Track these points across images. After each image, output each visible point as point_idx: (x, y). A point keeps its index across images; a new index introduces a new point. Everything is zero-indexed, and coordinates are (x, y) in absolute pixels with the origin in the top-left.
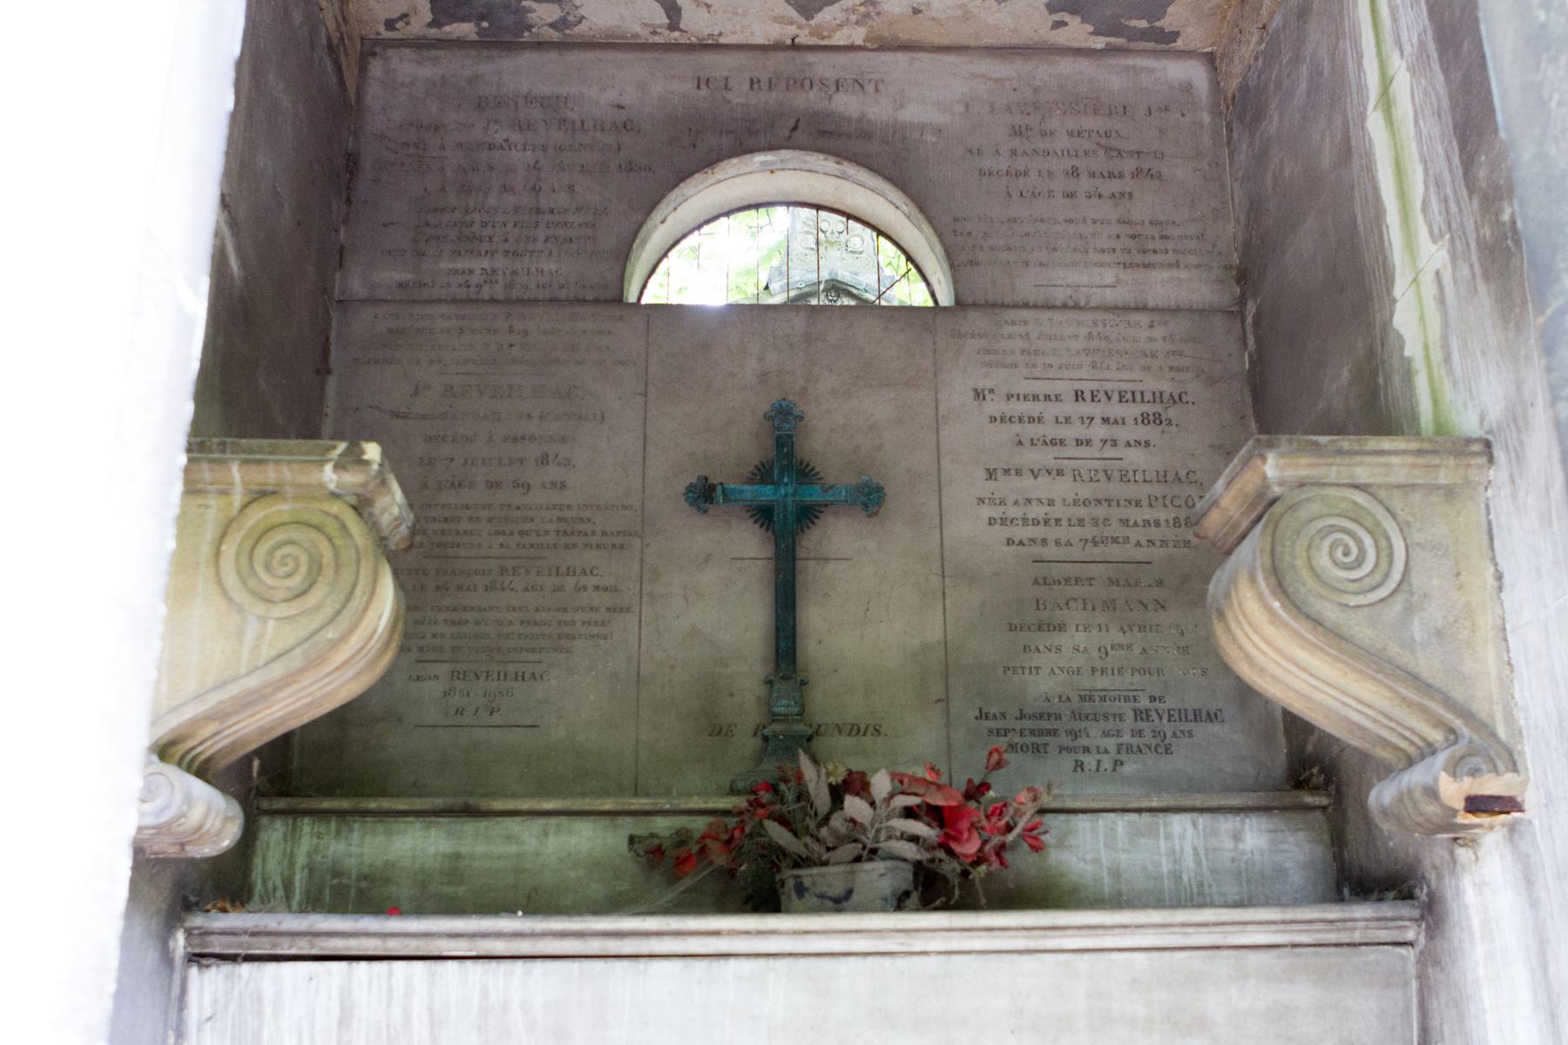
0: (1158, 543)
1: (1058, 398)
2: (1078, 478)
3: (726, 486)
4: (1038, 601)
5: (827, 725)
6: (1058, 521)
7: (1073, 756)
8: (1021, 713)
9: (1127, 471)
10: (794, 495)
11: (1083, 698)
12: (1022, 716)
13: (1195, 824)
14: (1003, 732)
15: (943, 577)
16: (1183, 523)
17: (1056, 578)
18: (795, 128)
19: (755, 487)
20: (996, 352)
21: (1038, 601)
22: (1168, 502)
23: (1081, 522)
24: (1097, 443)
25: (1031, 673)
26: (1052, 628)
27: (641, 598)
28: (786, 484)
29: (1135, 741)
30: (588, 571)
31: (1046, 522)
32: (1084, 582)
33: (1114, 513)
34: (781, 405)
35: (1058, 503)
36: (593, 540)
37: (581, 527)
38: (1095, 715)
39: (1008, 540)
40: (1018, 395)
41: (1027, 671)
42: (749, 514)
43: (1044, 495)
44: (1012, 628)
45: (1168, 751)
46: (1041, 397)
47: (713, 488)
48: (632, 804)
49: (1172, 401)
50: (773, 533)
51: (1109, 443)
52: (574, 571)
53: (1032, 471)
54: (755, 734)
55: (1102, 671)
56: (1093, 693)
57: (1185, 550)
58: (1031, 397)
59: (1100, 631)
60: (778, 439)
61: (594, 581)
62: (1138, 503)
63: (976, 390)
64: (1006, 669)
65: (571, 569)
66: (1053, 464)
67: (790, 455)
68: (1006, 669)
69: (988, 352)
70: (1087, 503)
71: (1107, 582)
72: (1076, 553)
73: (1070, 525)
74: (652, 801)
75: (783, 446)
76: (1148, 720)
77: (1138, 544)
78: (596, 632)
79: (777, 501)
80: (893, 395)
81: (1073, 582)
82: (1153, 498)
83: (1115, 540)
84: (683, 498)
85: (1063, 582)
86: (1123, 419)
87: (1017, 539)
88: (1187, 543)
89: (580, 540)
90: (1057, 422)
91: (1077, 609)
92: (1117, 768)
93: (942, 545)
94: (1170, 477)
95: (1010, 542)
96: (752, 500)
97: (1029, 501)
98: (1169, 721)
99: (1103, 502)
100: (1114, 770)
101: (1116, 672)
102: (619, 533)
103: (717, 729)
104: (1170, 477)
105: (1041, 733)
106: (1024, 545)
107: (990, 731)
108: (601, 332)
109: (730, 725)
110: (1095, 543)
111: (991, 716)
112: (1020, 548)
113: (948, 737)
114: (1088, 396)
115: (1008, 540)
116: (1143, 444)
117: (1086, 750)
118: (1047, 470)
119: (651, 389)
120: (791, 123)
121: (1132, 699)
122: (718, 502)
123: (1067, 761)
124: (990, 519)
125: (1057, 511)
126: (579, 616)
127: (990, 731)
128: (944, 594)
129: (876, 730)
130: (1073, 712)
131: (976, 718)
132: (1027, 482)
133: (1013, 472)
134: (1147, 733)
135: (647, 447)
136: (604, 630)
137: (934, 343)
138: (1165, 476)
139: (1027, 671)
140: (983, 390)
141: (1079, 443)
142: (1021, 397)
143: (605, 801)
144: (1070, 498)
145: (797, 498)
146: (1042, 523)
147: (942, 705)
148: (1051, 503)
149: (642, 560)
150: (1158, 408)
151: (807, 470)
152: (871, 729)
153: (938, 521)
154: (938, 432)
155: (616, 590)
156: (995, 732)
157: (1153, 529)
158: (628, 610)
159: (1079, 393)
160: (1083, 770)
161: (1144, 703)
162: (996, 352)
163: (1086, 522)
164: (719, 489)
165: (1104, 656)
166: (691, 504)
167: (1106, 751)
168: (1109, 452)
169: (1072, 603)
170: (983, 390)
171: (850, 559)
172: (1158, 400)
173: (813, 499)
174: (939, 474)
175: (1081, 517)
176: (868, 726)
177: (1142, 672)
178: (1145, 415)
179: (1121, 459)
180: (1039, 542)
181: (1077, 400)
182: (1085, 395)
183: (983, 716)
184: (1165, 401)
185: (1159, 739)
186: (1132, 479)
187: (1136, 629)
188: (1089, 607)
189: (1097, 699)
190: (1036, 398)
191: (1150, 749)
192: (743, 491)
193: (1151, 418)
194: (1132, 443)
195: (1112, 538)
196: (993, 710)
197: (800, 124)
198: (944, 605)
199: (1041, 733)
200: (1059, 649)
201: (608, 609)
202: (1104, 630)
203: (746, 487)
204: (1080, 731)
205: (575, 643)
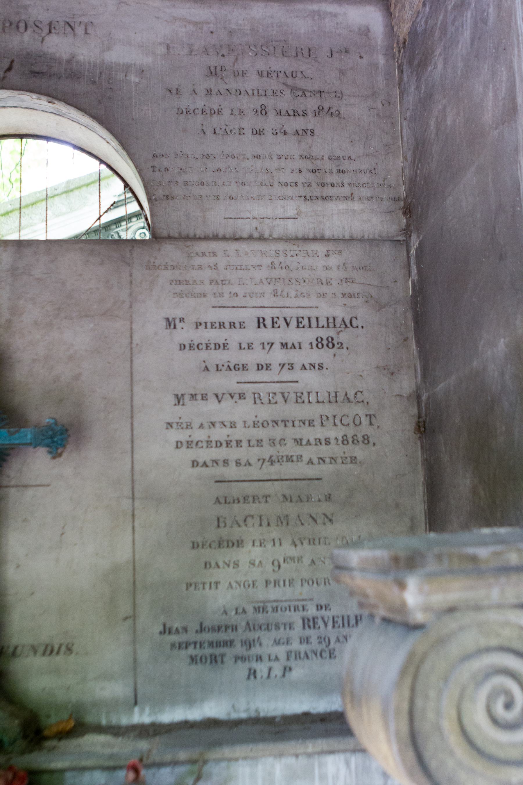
0: (327, 460)
1: (242, 325)
2: (258, 401)
4: (218, 519)
6: (239, 443)
7: (247, 665)
9: (302, 393)
11: (257, 610)
12: (202, 629)
13: (347, 763)
14: (184, 645)
15: (133, 499)
16: (350, 441)
17: (236, 497)
18: (9, 69)
20: (187, 282)
21: (218, 519)
22: (338, 422)
23: (259, 442)
24: (275, 367)
26: (231, 544)
29: (303, 648)
32: (261, 500)
33: (290, 433)
35: (239, 425)
38: (268, 625)
39: (193, 462)
40: (206, 323)
41: (207, 586)
43: (227, 419)
44: (195, 546)
45: (332, 655)
46: (227, 325)
49: (344, 326)
51: (286, 366)
53: (217, 396)
56: (266, 604)
57: (352, 466)
58: (217, 325)
59: (274, 545)
62: (311, 423)
63: (167, 319)
64: (189, 585)
66: (236, 388)
68: (189, 585)
69: (180, 283)
70: (265, 424)
71: (281, 498)
72: (254, 473)
73: (250, 446)
76: (314, 627)
77: (310, 462)
80: (92, 325)
81: (251, 499)
82: (324, 418)
83: (290, 459)
85: (242, 500)
86: (300, 344)
87: (201, 461)
88: (354, 460)
90: (240, 348)
91: (253, 525)
92: (286, 674)
94: (340, 397)
95: (195, 464)
97: (213, 424)
98: (334, 627)
99: (280, 423)
100: (284, 675)
101: (287, 583)
104: (340, 397)
105: (219, 644)
106: (207, 466)
107: (173, 645)
110: (272, 462)
111: (174, 630)
112: (204, 469)
113: (135, 652)
114: (268, 322)
115: (193, 462)
116: (317, 367)
117: (259, 658)
118: (230, 394)
120: (6, 64)
121: (301, 608)
123: (242, 669)
124: (177, 442)
125: (238, 433)
127: (173, 645)
128: (133, 515)
130: (248, 624)
132: (212, 405)
133: (199, 397)
134: (314, 640)
137: (131, 275)
138: (336, 397)
139: (207, 586)
140: (174, 319)
141: (260, 367)
142: (209, 325)
144: (251, 419)
146: (224, 444)
147: (130, 621)
148: (233, 425)
150: (331, 332)
152: (63, 648)
153: (129, 446)
154: (131, 361)
156: (177, 645)
157: (324, 447)
159: (261, 320)
161: (312, 611)
162: (187, 282)
163: (264, 443)
165: (276, 569)
167: (277, 659)
168: (286, 375)
169: (249, 520)
170: (174, 319)
172: (331, 325)
174: (132, 401)
175: (259, 438)
177: (311, 583)
178: (319, 340)
179: (297, 382)
180: (221, 463)
181: (259, 327)
182: (266, 322)
183: (166, 630)
184: (338, 325)
185: (324, 645)
186: (306, 400)
187: (306, 542)
188: (265, 523)
189: (270, 609)
190: (222, 325)
191: (316, 654)
193: (325, 342)
194: (307, 366)
195: (287, 456)
196: (176, 625)
197: (14, 64)
198: (133, 528)
199: (219, 644)
200: (236, 565)
202: (277, 544)
204: (254, 641)
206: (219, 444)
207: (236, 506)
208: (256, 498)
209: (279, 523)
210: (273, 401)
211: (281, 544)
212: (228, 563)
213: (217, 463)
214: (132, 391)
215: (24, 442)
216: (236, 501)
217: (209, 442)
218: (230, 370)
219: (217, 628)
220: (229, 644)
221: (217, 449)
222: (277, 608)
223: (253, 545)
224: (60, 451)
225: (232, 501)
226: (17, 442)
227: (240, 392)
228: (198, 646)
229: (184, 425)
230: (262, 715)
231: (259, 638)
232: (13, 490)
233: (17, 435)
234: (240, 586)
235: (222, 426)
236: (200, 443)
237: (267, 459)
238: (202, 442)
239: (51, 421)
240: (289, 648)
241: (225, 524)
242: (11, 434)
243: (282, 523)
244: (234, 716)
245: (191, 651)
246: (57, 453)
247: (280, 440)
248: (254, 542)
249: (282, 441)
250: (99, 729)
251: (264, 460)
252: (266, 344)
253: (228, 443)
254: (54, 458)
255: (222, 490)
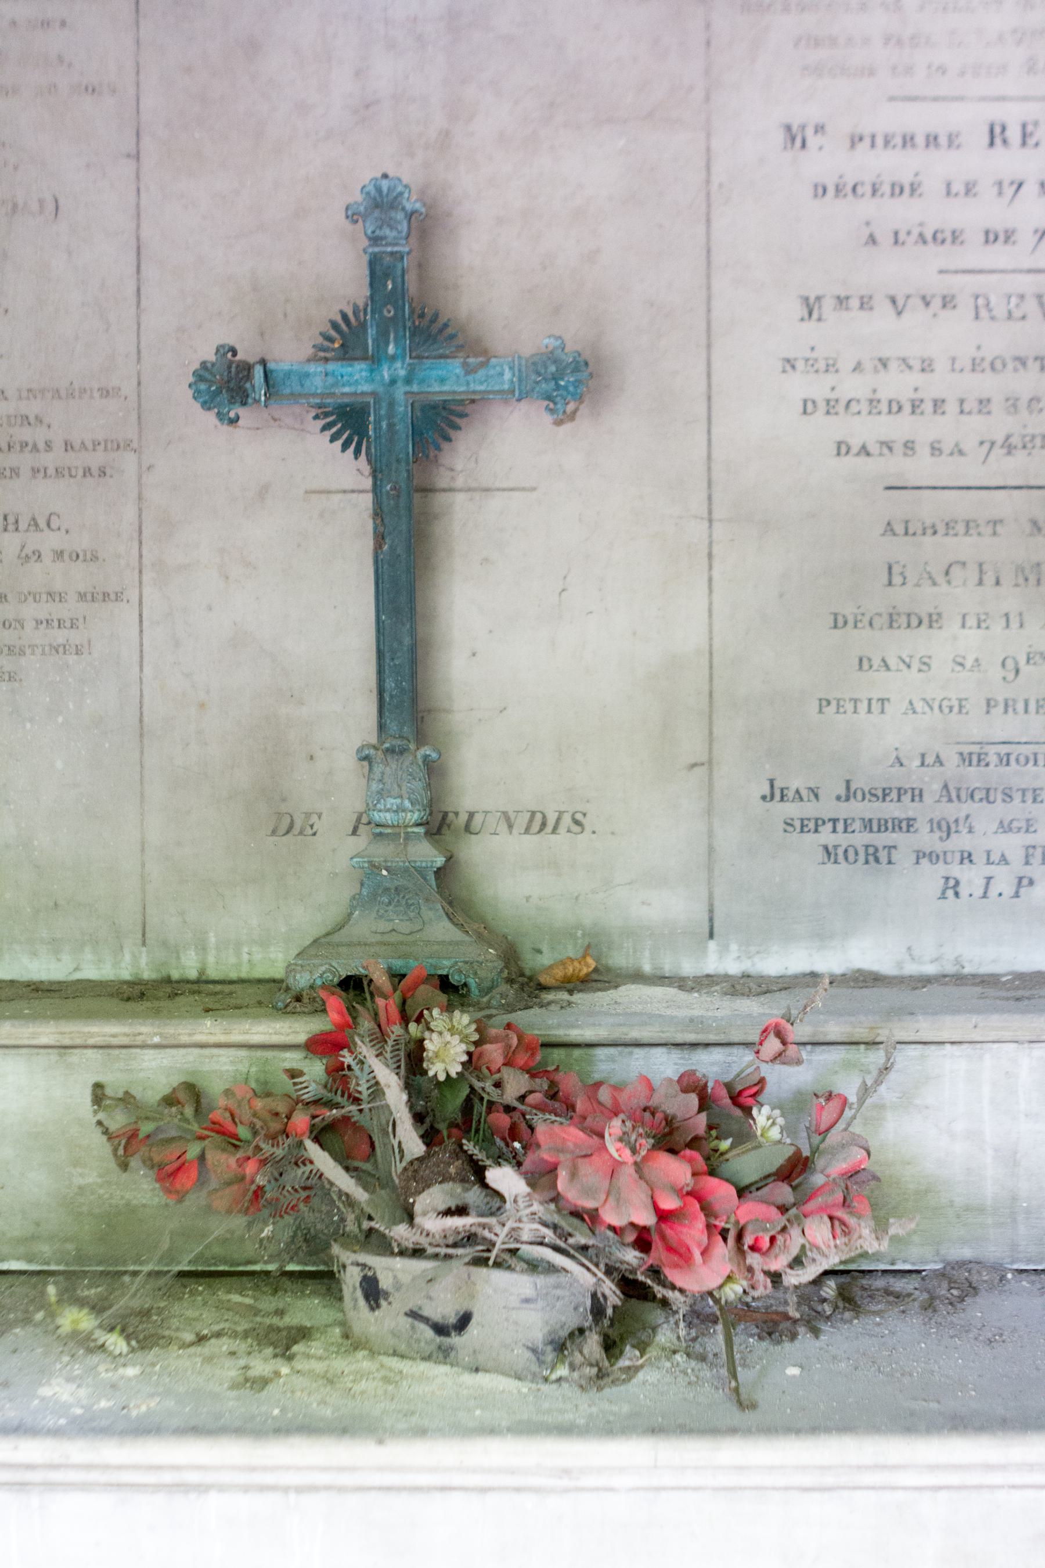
1: (953, 141)
2: (983, 313)
3: (271, 366)
4: (890, 568)
5: (486, 812)
6: (938, 405)
7: (941, 869)
8: (848, 788)
10: (408, 381)
11: (966, 759)
12: (849, 794)
15: (710, 521)
17: (928, 523)
19: (331, 366)
20: (833, 41)
21: (890, 568)
23: (984, 403)
25: (869, 711)
26: (914, 622)
27: (140, 572)
28: (393, 358)
30: (42, 524)
31: (915, 406)
32: (982, 529)
34: (379, 190)
36: (49, 460)
37: (26, 434)
38: (988, 790)
39: (839, 444)
40: (873, 137)
41: (863, 707)
42: (321, 423)
44: (838, 622)
46: (920, 140)
47: (247, 368)
48: (91, 1035)
50: (369, 461)
52: (17, 522)
53: (893, 301)
54: (355, 832)
55: (1006, 706)
56: (988, 748)
58: (898, 140)
59: (1008, 626)
60: (374, 263)
61: (49, 541)
63: (788, 128)
65: (11, 519)
66: (939, 285)
67: (397, 297)
69: (817, 43)
70: (998, 365)
71: (1028, 528)
72: (971, 471)
73: (962, 412)
74: (126, 1029)
75: (386, 276)
78: (61, 641)
79: (374, 394)
80: (622, 143)
81: (961, 528)
84: (190, 393)
87: (856, 445)
89: (25, 461)
90: (948, 193)
91: (964, 584)
92: (1022, 891)
93: (709, 457)
95: (842, 448)
96: (322, 395)
97: (884, 363)
99: (1030, 363)
100: (1017, 895)
101: (1032, 707)
102: (96, 444)
103: (286, 822)
105: (883, 826)
106: (868, 454)
108: (46, 24)
109: (308, 815)
110: (1010, 449)
111: (791, 794)
112: (862, 459)
113: (711, 834)
114: (1014, 134)
115: (839, 444)
117: (967, 858)
118: (924, 298)
119: (146, 142)
122: (258, 401)
123: (931, 877)
124: (805, 402)
125: (935, 385)
126: (30, 611)
128: (710, 555)
129: (577, 823)
130: (946, 786)
131: (764, 798)
132: (883, 318)
133: (855, 303)
135: (143, 267)
136: (75, 637)
137: (708, 26)
139: (863, 707)
140: (803, 127)
141: (990, 237)
142: (880, 141)
143: (40, 1030)
145: (415, 388)
146: (907, 408)
148: (927, 366)
149: (140, 498)
151: (434, 329)
152: (567, 820)
153: (701, 410)
154: (708, 221)
155: (95, 558)
158: (118, 596)
159: (997, 130)
160: (957, 894)
162: (833, 41)
163: (994, 407)
164: (258, 372)
165: (1011, 676)
166: (206, 406)
167: (1004, 860)
169: (955, 571)
170: (803, 127)
171: (534, 489)
173: (446, 388)
174: (709, 311)
175: (984, 396)
176: (561, 813)
180: (898, 448)
181: (992, 144)
182: (1008, 133)
183: (775, 793)
188: (989, 578)
189: (993, 759)
190: (908, 141)
192: (307, 375)
196: (795, 783)
198: (710, 580)
199: (883, 826)
200: (925, 664)
201: (82, 596)
202: (1014, 624)
203: (312, 368)
204: (957, 821)
205: (23, 661)
206: (895, 408)
207: (928, 539)
208: (972, 524)
209: (1021, 580)
210: (1017, 314)
211: (1021, 626)
212: (907, 660)
213: (890, 449)
214: (709, 288)
215: (497, 388)
216: (929, 531)
217: (875, 403)
218: (925, 242)
219: (880, 793)
220: (904, 825)
221: (891, 417)
222: (1008, 755)
223: (963, 626)
224: (571, 407)
225: (919, 531)
226: (482, 388)
227: (945, 292)
228: (840, 826)
229: (821, 365)
230: (968, 970)
231: (967, 817)
232: (460, 498)
233: (481, 373)
234: (931, 708)
235: (903, 367)
236: (853, 404)
237: (1000, 443)
238: (858, 401)
239: (553, 343)
240: (1030, 839)
241: (905, 578)
242: (469, 370)
243: (1026, 580)
244: (912, 969)
245: (826, 836)
246: (564, 412)
247: (1031, 400)
248: (964, 617)
249: (1034, 402)
250: (638, 977)
251: (993, 444)
252: (1006, 184)
253: (915, 406)
254: (559, 423)
255: (899, 506)
